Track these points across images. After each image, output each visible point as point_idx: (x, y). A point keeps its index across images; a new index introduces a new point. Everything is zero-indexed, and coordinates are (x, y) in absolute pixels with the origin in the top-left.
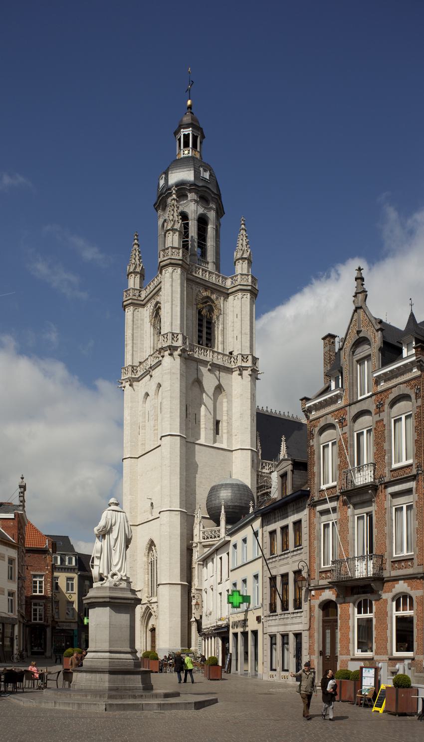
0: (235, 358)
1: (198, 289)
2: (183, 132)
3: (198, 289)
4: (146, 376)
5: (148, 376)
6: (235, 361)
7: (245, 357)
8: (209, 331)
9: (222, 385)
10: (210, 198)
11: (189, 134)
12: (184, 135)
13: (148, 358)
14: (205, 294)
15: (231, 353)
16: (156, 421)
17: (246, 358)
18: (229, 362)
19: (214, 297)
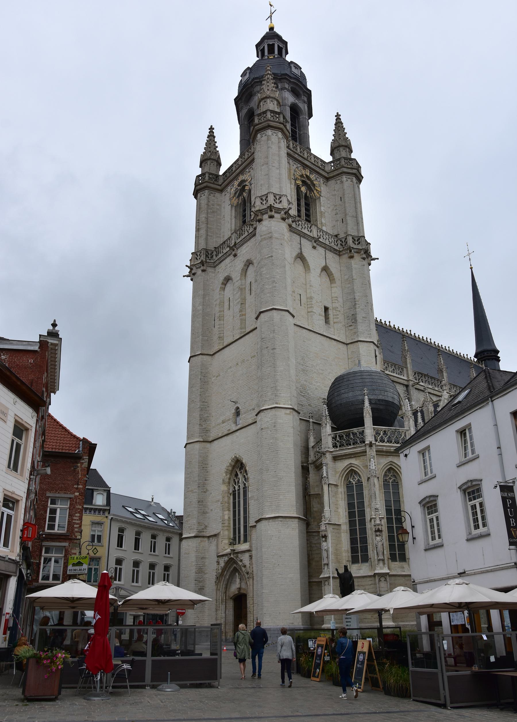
0: (343, 240)
1: (295, 166)
2: (267, 42)
3: (295, 166)
4: (229, 255)
5: (231, 257)
6: (344, 244)
7: (356, 239)
8: (307, 213)
9: (330, 267)
10: (301, 93)
11: (273, 45)
12: (269, 45)
13: (231, 237)
14: (304, 172)
15: (336, 236)
16: (243, 305)
17: (358, 240)
18: (336, 244)
19: (313, 177)
